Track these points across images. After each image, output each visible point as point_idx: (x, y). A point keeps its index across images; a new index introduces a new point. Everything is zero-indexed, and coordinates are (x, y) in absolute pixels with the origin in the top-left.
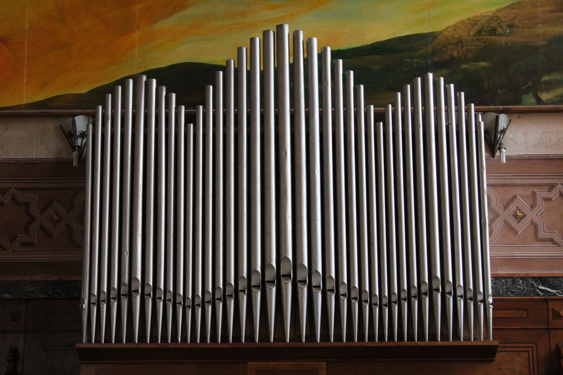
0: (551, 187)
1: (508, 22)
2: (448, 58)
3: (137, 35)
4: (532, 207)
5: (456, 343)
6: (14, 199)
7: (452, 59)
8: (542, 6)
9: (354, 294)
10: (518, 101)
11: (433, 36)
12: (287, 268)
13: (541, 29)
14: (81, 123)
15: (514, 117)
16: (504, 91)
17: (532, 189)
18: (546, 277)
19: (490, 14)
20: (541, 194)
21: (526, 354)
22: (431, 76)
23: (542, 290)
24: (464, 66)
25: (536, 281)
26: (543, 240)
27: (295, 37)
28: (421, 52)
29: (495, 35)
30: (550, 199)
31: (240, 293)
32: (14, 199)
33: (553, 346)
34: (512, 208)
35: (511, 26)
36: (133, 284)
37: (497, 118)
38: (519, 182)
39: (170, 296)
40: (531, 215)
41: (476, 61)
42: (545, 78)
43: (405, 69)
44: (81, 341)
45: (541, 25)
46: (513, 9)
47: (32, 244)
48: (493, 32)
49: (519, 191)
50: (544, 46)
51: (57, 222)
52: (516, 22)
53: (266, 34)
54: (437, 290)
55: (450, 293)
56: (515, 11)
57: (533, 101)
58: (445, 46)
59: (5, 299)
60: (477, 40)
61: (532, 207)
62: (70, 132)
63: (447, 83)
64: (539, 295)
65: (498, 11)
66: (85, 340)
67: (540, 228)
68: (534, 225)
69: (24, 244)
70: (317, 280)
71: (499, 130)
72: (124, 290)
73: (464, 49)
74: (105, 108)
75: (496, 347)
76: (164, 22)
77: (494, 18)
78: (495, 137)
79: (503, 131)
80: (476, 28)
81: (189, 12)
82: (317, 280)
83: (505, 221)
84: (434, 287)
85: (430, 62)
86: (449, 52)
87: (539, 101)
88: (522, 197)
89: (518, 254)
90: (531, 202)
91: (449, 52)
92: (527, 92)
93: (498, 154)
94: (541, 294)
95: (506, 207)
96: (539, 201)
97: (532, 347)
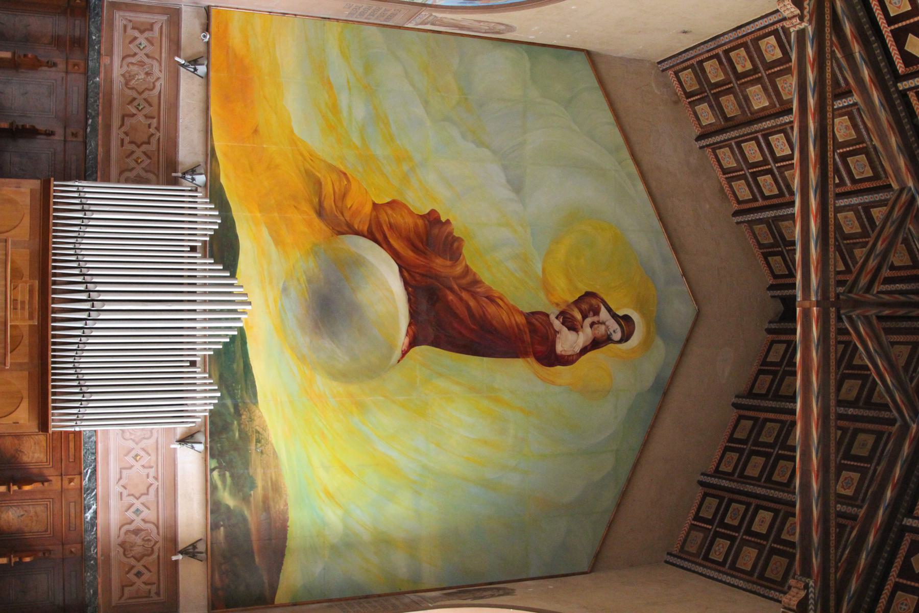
0: (156, 478)
1: (264, 452)
2: (241, 412)
3: (258, 215)
4: (143, 466)
5: (50, 408)
6: (152, 135)
7: (240, 415)
8: (275, 472)
9: (81, 347)
10: (212, 456)
11: (256, 403)
12: (98, 305)
13: (260, 471)
14: (200, 179)
15: (202, 455)
16: (219, 448)
17: (155, 466)
18: (96, 474)
19: (270, 439)
20: (152, 472)
21: (45, 461)
22: (219, 394)
23: (87, 472)
24: (235, 422)
25: (93, 468)
26: (121, 472)
27: (244, 313)
28: (245, 395)
29: (256, 442)
30: (148, 477)
31: (83, 277)
32: (152, 135)
33: (50, 478)
34: (142, 453)
35: (262, 452)
36: (90, 213)
37: (201, 443)
38: (160, 458)
39: (82, 235)
40: (138, 466)
41: (239, 430)
42: (227, 474)
43: (234, 385)
44: (55, 180)
45: (262, 471)
46: (273, 455)
47: (122, 145)
48: (258, 441)
49: (153, 458)
50: (248, 474)
51: (137, 162)
52: (264, 456)
53: (246, 295)
54: (83, 397)
55: (81, 404)
56: (272, 455)
57: (213, 467)
58: (249, 410)
59: (86, 129)
60: (253, 431)
61: (143, 466)
62: (195, 171)
63: (214, 404)
64: (84, 469)
65: (272, 445)
66: (55, 183)
67: (128, 471)
68: (131, 467)
69: (122, 140)
70: (90, 324)
71: (194, 445)
72: (86, 207)
73: (247, 423)
74: (201, 198)
75: (48, 432)
76: (267, 233)
77: (268, 442)
78: (188, 442)
79: (193, 448)
80: (260, 430)
81: (273, 248)
82: (90, 324)
83: (134, 448)
84: (85, 395)
85: (239, 401)
86: (245, 413)
87: (212, 470)
88: (150, 459)
89: (112, 457)
90: (146, 465)
91: (245, 413)
92: (219, 462)
93: (178, 443)
94: (85, 471)
95: (143, 449)
96: (147, 471)
97: (50, 464)
